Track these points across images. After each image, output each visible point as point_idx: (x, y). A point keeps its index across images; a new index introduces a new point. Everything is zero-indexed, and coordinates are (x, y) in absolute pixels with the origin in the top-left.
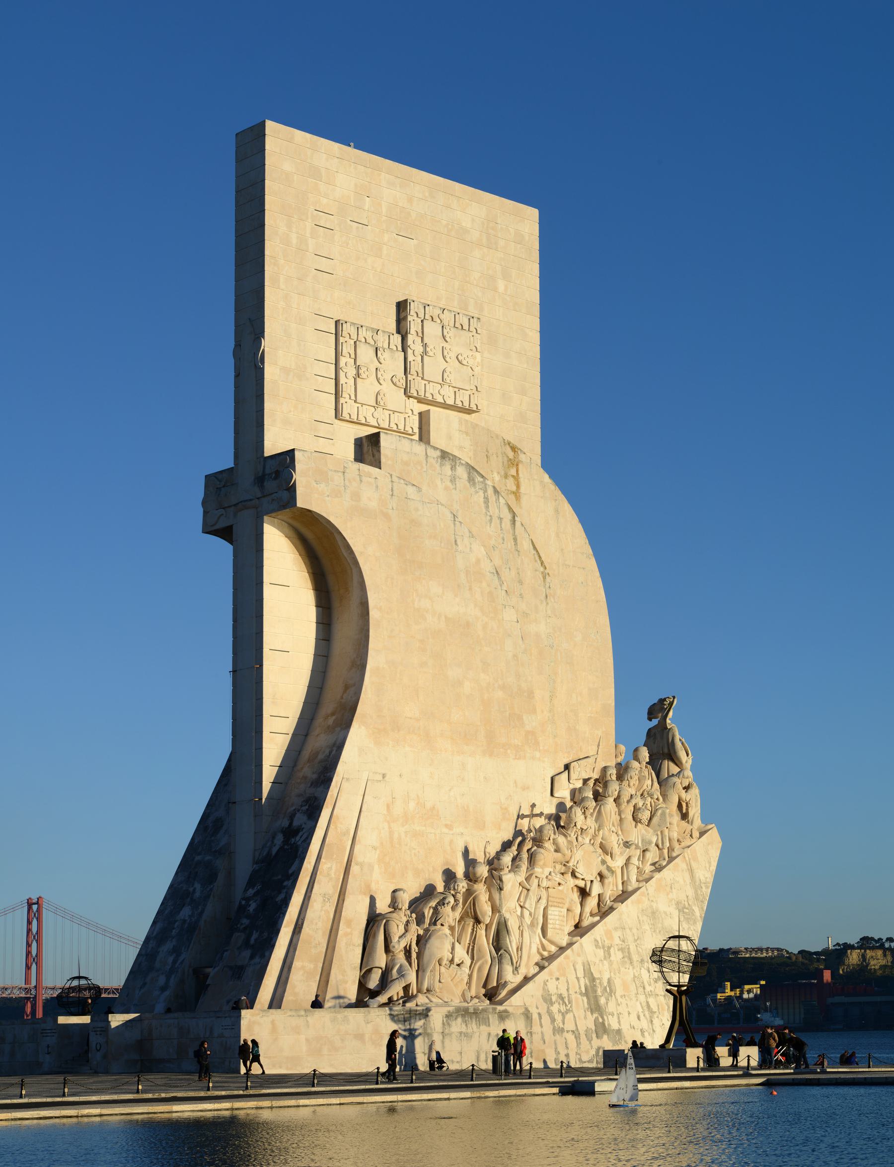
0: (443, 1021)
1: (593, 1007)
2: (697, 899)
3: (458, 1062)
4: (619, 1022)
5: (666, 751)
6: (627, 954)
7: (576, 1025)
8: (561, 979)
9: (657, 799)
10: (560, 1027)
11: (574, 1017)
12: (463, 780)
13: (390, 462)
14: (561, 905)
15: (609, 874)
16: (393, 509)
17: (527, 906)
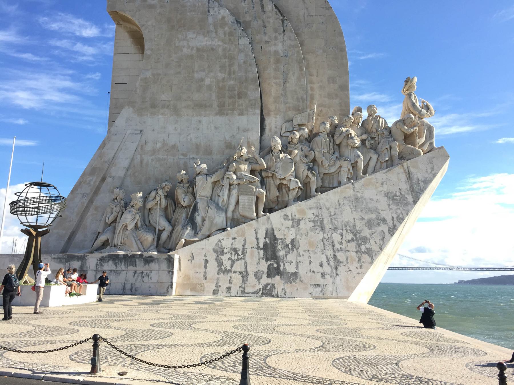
0: (97, 262)
1: (269, 257)
2: (412, 190)
4: (297, 268)
5: (407, 108)
6: (319, 224)
7: (246, 268)
8: (238, 238)
9: (383, 134)
10: (226, 269)
11: (246, 262)
12: (198, 129)
14: (249, 194)
15: (312, 176)
16: (167, 2)
17: (220, 195)
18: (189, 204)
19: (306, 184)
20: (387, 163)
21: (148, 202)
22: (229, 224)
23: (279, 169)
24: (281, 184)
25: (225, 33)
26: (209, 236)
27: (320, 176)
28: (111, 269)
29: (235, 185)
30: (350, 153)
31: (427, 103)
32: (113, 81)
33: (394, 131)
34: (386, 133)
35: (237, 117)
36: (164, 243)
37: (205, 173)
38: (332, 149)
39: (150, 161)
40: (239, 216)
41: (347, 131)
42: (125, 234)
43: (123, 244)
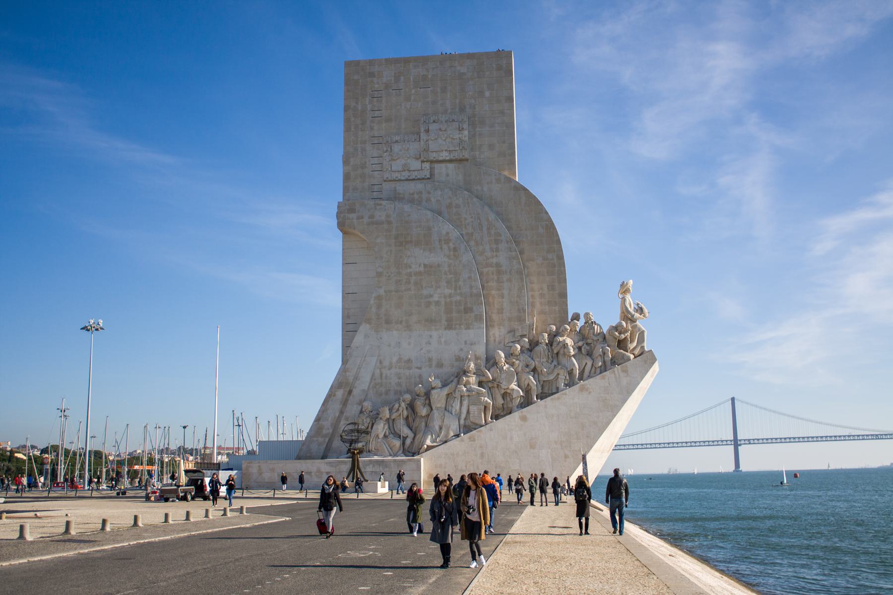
9: (598, 340)
12: (430, 344)
13: (402, 196)
14: (478, 404)
17: (454, 405)
19: (527, 391)
22: (462, 430)
24: (506, 392)
25: (450, 250)
26: (446, 442)
33: (607, 336)
34: (601, 339)
36: (409, 447)
39: (389, 375)
40: (470, 422)
41: (564, 340)
42: (378, 442)
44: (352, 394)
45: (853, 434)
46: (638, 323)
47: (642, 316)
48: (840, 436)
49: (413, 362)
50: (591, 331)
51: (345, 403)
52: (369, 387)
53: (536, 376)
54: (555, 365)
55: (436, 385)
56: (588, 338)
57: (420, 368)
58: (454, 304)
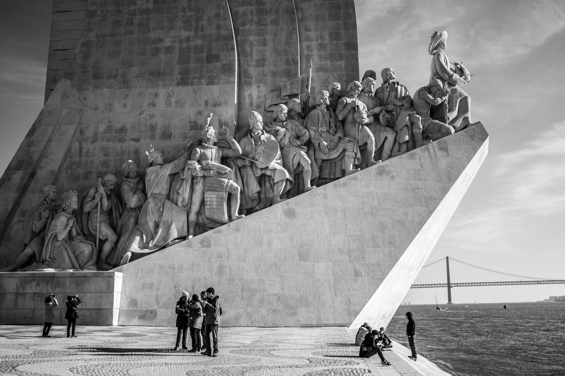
0: (17, 284)
3: (30, 318)
5: (435, 72)
9: (403, 106)
12: (154, 105)
14: (219, 189)
17: (180, 191)
18: (139, 205)
20: (407, 145)
21: (85, 204)
22: (191, 230)
23: (259, 155)
26: (164, 247)
27: (316, 164)
28: (35, 292)
29: (199, 178)
30: (357, 132)
31: (461, 66)
32: (50, 47)
33: (416, 101)
34: (407, 105)
35: (206, 87)
36: (108, 256)
37: (160, 163)
38: (334, 127)
39: (91, 150)
42: (55, 247)
43: (53, 259)
44: (35, 178)
45: (523, 281)
46: (457, 87)
47: (462, 79)
48: (515, 282)
49: (128, 131)
50: (393, 94)
51: (23, 190)
52: (60, 168)
53: (311, 152)
54: (340, 138)
55: (153, 159)
56: (388, 104)
57: (137, 140)
58: (192, 50)
